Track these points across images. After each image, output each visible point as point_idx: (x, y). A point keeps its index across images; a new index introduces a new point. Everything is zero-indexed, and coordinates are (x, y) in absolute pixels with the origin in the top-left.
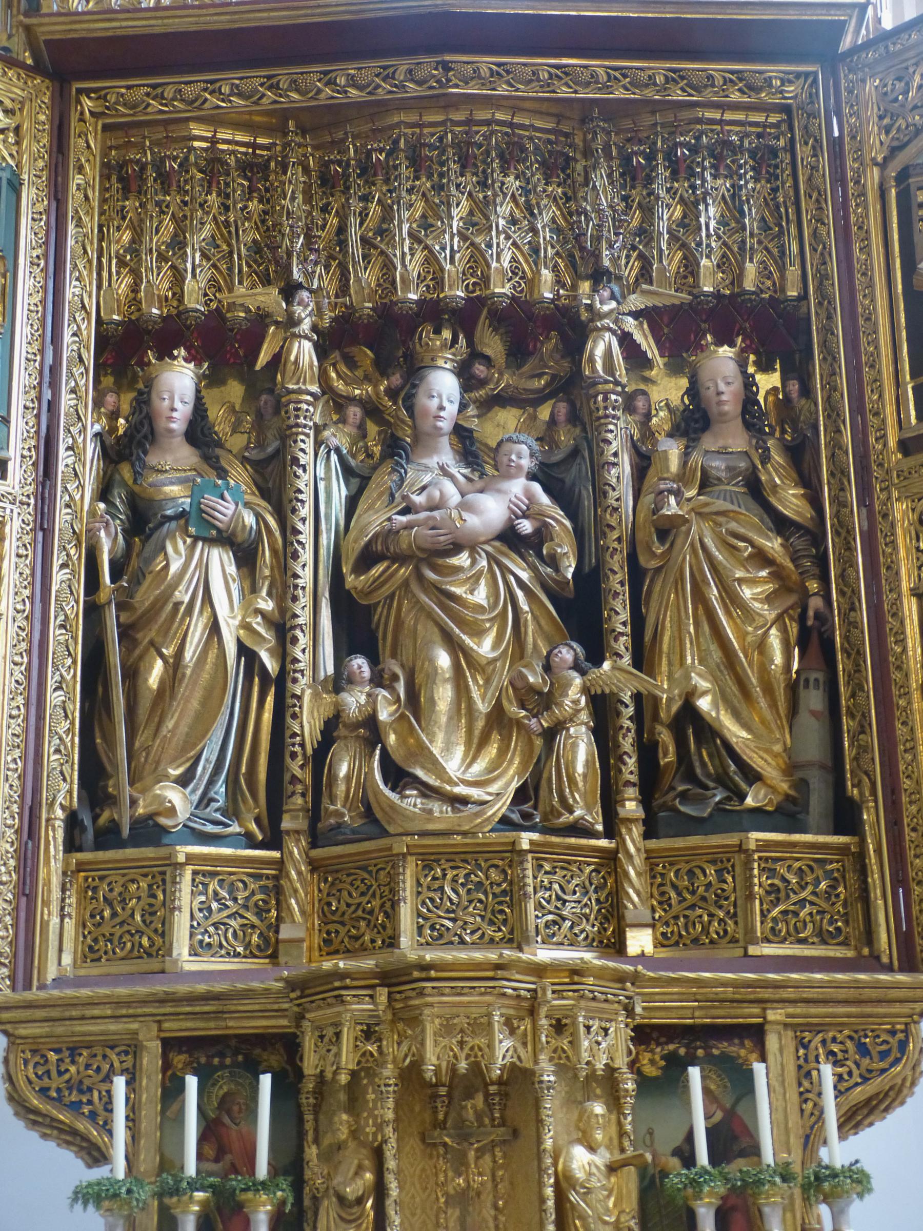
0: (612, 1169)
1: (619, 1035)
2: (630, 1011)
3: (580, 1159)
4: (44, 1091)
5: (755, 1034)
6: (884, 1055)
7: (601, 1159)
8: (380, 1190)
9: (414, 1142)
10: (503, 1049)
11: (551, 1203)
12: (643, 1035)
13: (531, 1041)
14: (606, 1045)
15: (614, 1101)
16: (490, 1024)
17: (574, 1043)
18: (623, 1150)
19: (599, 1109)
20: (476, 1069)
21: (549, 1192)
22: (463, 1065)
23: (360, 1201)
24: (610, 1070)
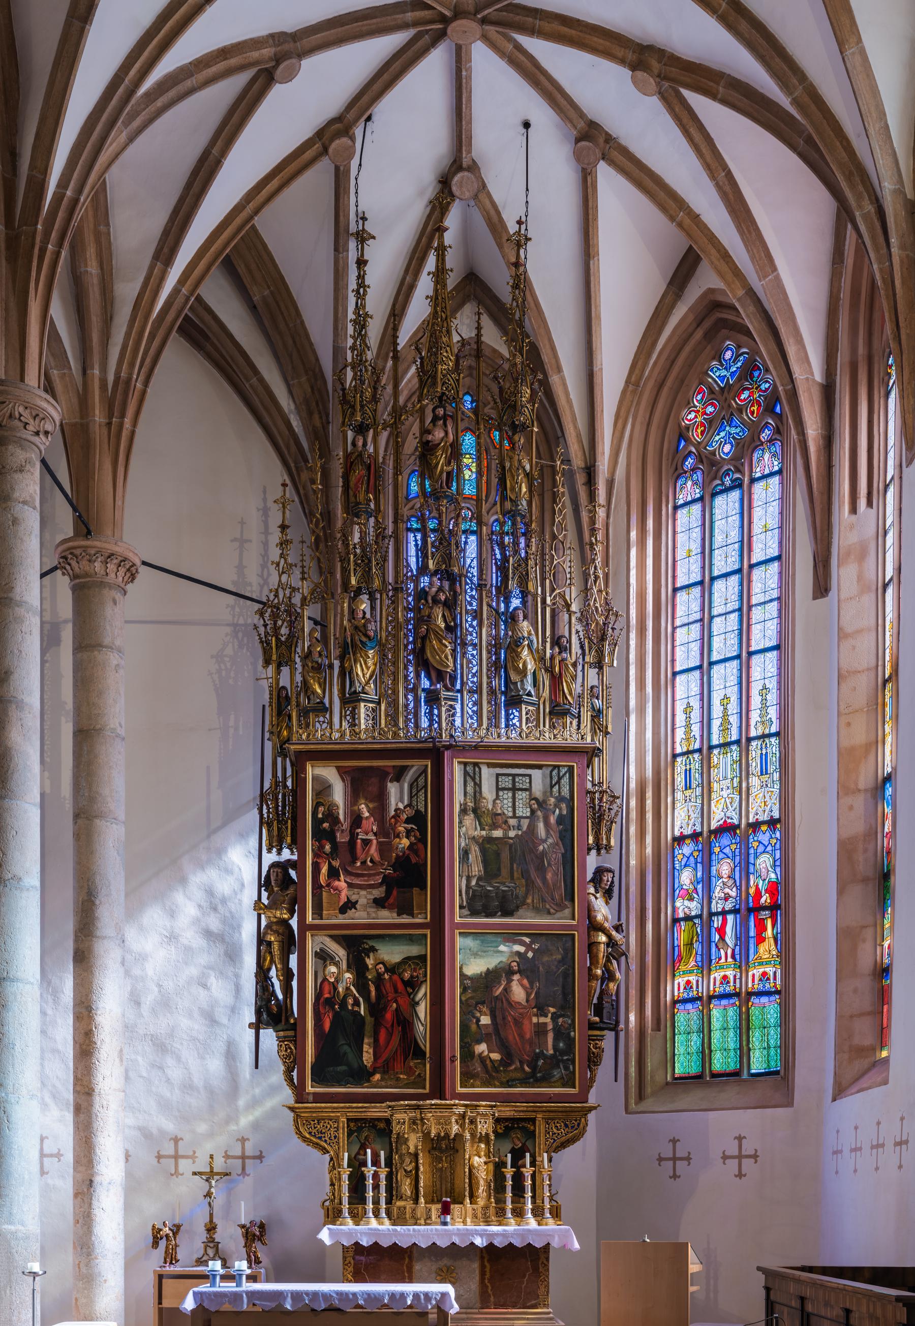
0: (486, 1163)
1: (490, 1121)
2: (494, 1115)
3: (476, 1160)
4: (310, 1133)
5: (533, 1121)
6: (572, 1127)
7: (483, 1159)
8: (417, 1168)
9: (427, 1154)
10: (455, 1129)
11: (467, 1174)
12: (498, 1121)
13: (462, 1126)
14: (485, 1127)
15: (488, 1143)
16: (451, 1122)
17: (476, 1127)
18: (489, 1157)
19: (483, 1146)
20: (447, 1135)
21: (467, 1170)
22: (442, 1134)
23: (411, 1171)
24: (487, 1135)
